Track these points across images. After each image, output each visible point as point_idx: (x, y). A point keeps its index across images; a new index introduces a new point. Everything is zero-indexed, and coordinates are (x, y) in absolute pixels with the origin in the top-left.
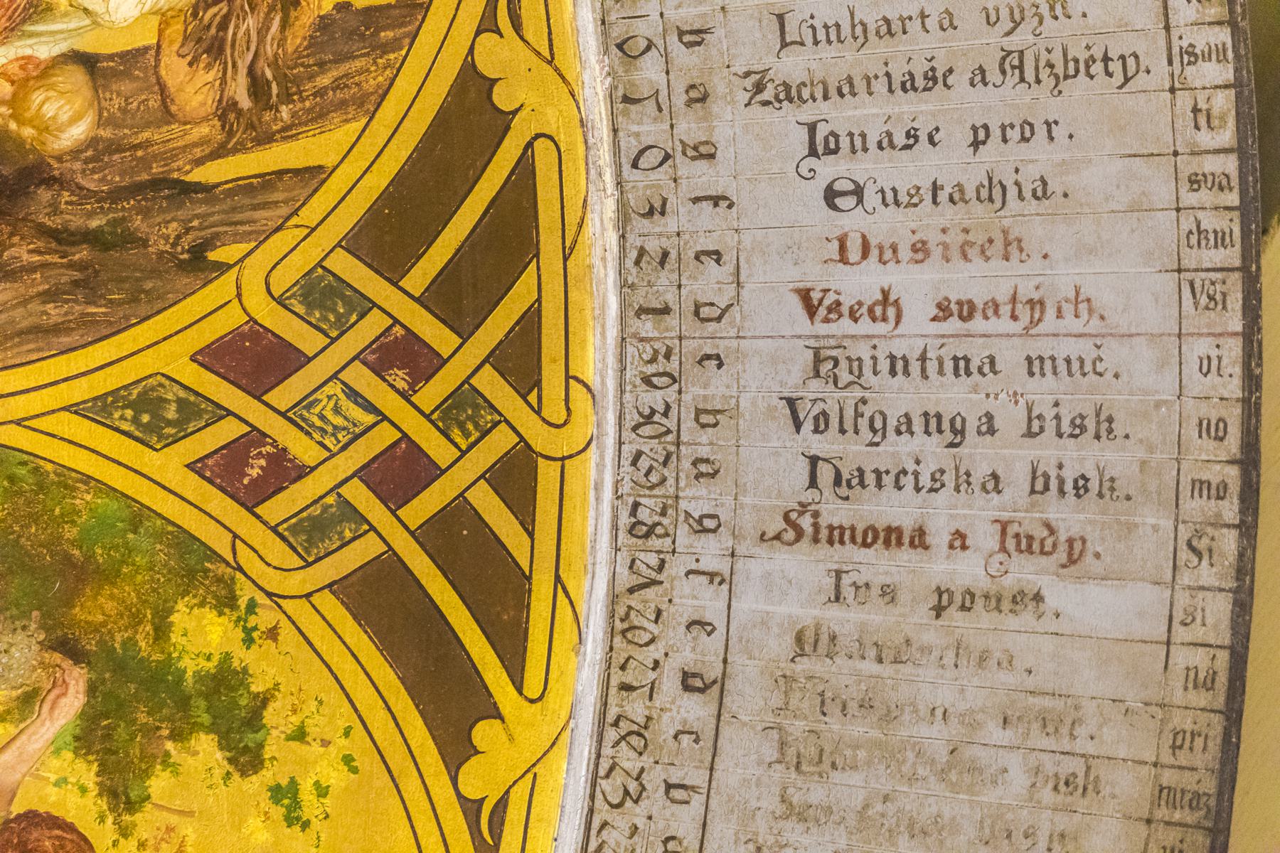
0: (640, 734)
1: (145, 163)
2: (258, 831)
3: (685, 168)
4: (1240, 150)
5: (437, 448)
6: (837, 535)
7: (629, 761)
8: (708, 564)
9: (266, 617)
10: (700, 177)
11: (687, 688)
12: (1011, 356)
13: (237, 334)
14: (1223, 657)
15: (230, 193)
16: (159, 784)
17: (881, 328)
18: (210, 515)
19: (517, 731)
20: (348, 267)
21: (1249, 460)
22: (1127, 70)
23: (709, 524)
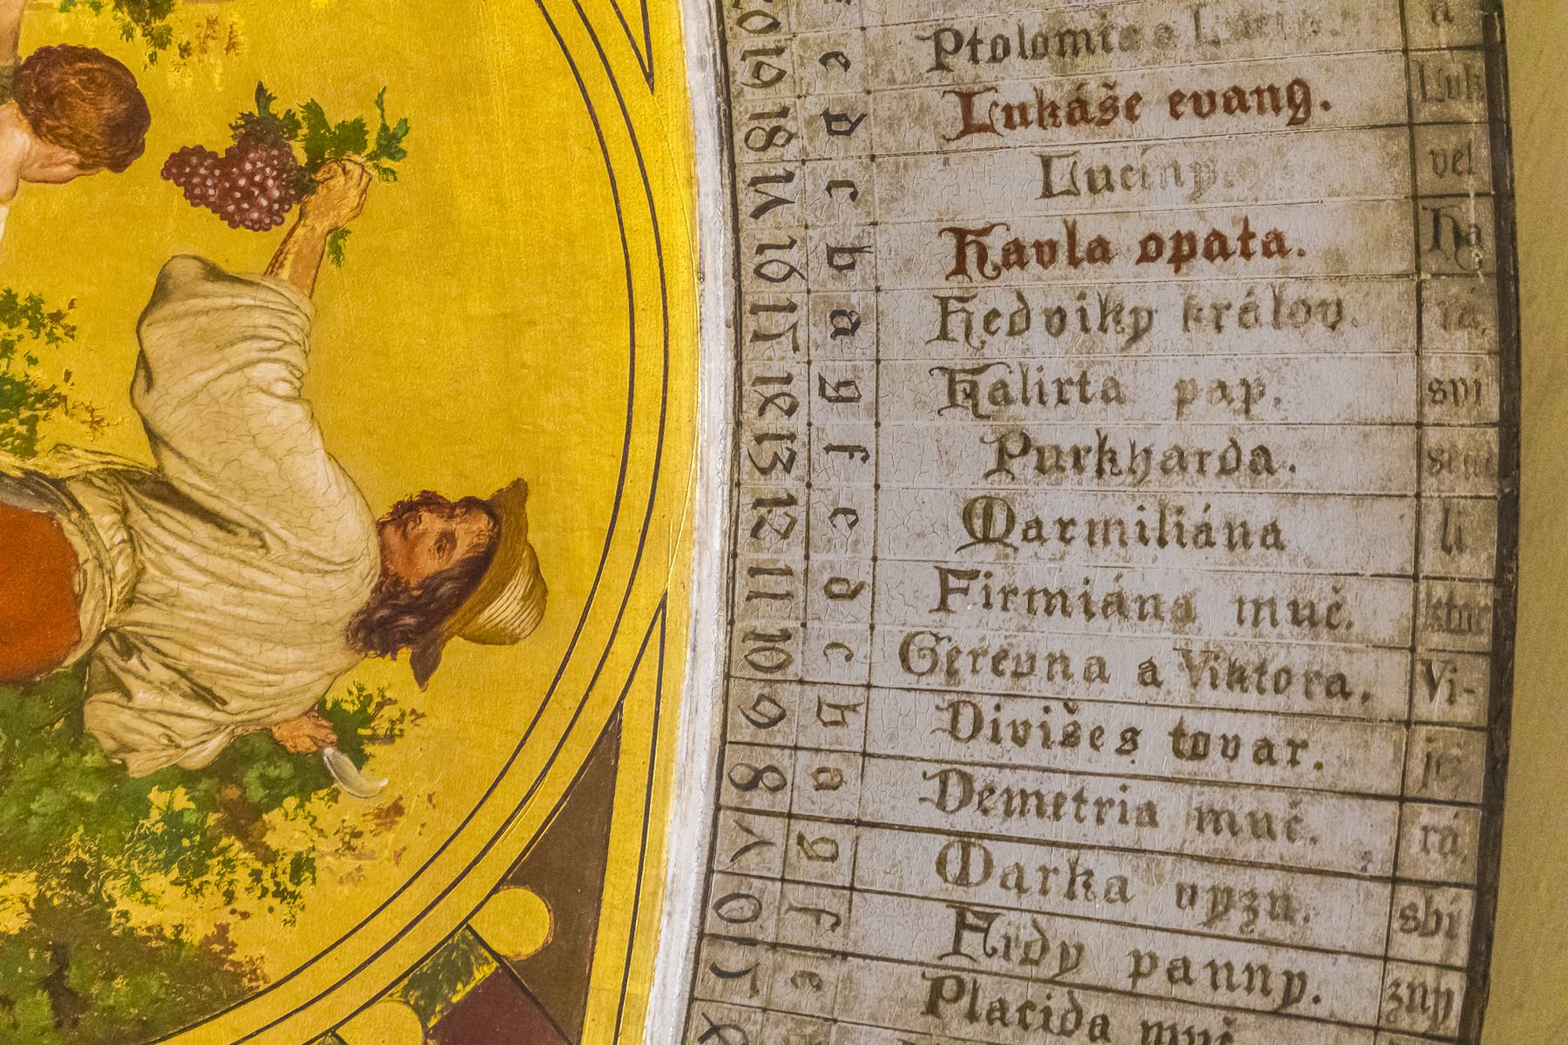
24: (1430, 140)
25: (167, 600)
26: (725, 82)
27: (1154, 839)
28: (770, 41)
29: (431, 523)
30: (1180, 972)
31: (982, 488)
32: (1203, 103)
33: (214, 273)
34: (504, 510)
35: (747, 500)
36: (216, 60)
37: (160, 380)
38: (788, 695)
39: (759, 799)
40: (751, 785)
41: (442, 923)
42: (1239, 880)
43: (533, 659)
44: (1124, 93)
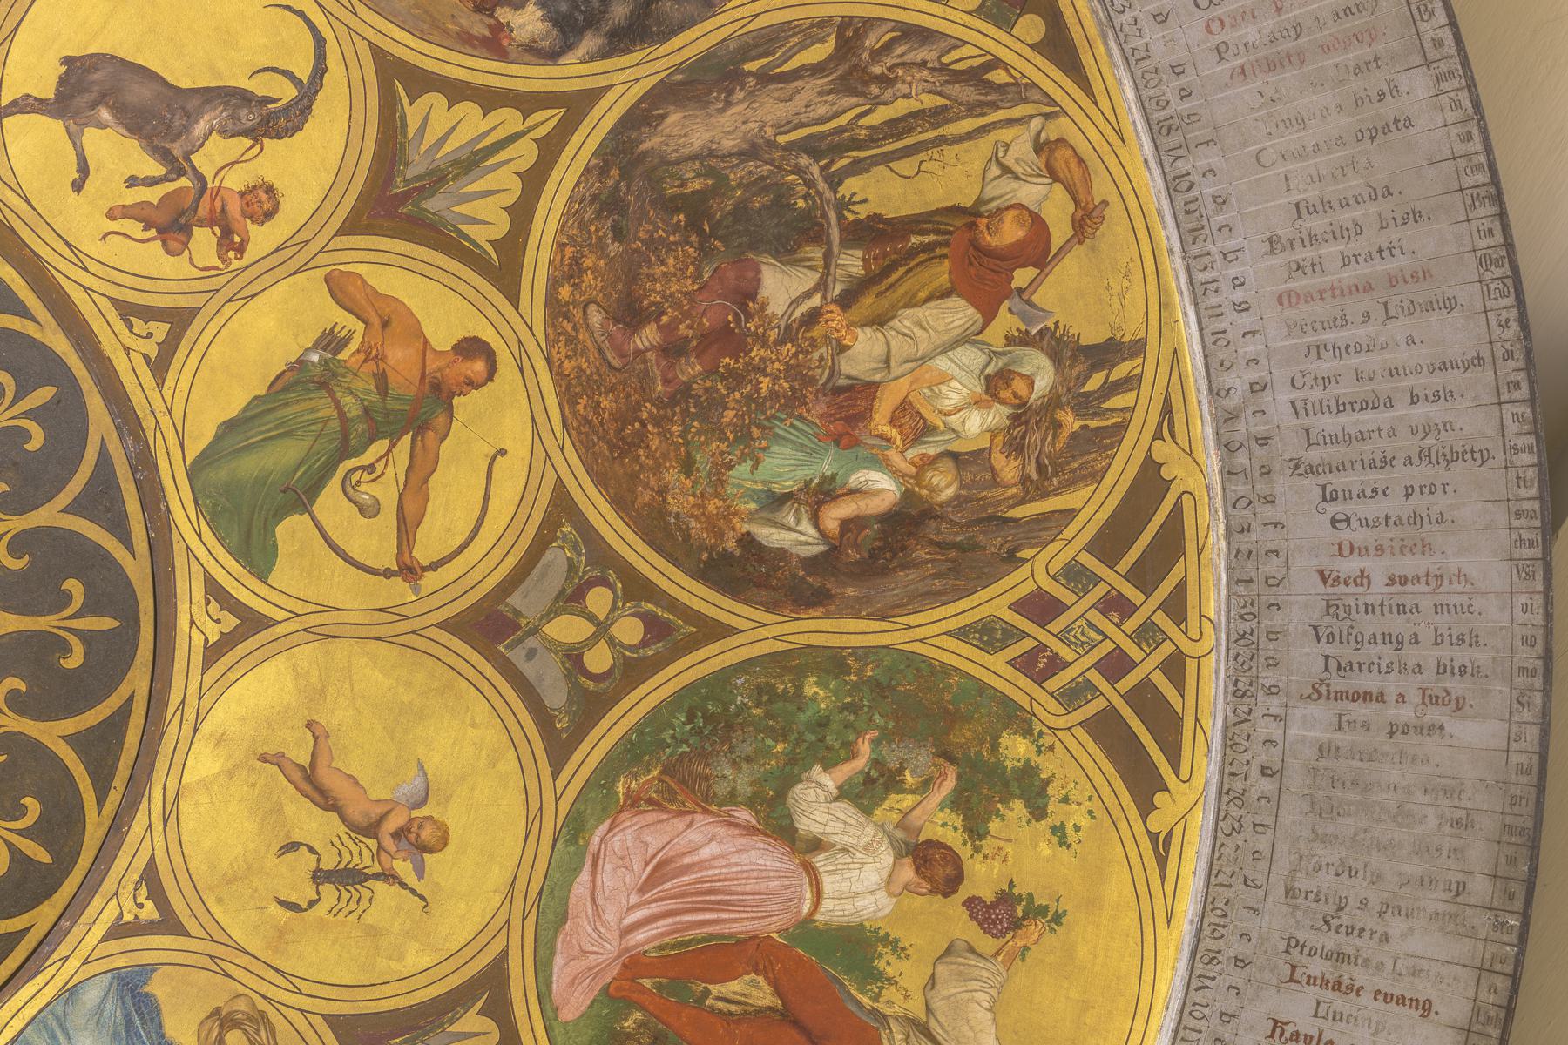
0: (1240, 798)
1: (984, 508)
2: (1045, 849)
4: (1541, 498)
5: (1134, 652)
6: (1339, 696)
7: (1235, 812)
8: (1273, 711)
9: (1047, 740)
10: (1267, 512)
11: (1263, 774)
12: (1426, 603)
13: (1032, 595)
14: (1536, 758)
16: (994, 825)
17: (1360, 590)
18: (1018, 687)
19: (1177, 797)
20: (1086, 559)
21: (1547, 656)
22: (1484, 458)
23: (1274, 690)
26: (1199, 932)
28: (1222, 921)
32: (1388, 997)
33: (971, 950)
36: (997, 864)
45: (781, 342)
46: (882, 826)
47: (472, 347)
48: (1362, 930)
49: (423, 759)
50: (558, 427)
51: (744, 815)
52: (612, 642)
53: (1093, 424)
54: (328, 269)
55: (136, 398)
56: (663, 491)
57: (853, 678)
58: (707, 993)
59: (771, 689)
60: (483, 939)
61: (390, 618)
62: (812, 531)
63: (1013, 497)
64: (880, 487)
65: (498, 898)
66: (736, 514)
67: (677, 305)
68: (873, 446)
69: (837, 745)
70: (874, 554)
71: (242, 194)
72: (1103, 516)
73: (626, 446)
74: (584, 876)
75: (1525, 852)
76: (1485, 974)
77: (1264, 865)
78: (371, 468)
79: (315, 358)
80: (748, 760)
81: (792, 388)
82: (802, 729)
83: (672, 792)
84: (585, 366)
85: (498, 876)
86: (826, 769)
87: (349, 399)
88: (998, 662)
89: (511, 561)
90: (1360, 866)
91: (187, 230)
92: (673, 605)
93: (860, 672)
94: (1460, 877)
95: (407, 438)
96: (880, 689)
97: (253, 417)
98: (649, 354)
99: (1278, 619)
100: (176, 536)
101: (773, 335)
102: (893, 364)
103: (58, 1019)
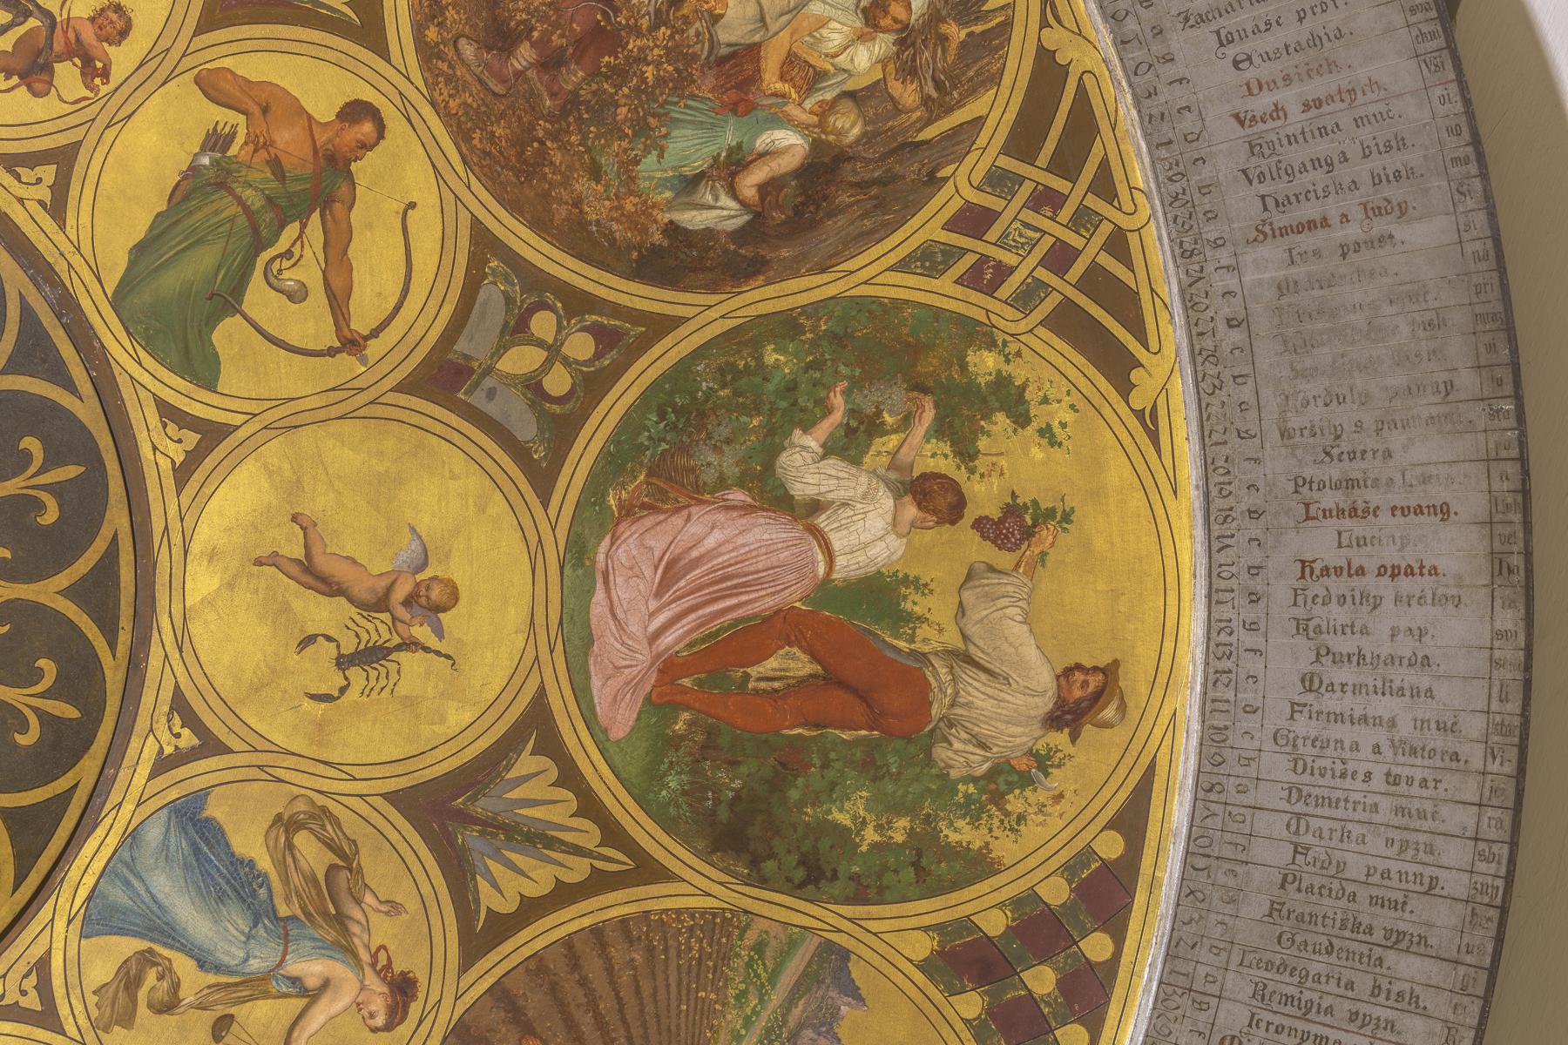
0: (1213, 355)
2: (1037, 454)
3: (1161, 69)
5: (1075, 241)
6: (1284, 231)
7: (1212, 370)
8: (1224, 262)
9: (1013, 347)
10: (1169, 71)
11: (1230, 326)
12: (1346, 120)
13: (961, 210)
14: (1489, 243)
15: (939, 142)
16: (983, 443)
17: (1279, 123)
18: (971, 304)
20: (1005, 162)
21: (1476, 141)
24: (1499, 529)
25: (968, 705)
26: (1207, 495)
27: (1377, 818)
28: (1226, 479)
29: (1079, 677)
30: (1386, 874)
31: (1310, 669)
32: (1405, 511)
33: (991, 569)
34: (1109, 673)
35: (1211, 670)
36: (995, 480)
37: (968, 613)
38: (1227, 753)
39: (1213, 796)
40: (1210, 790)
41: (1079, 844)
42: (1412, 837)
43: (1119, 735)
44: (1372, 506)
45: (655, 27)
46: (874, 472)
47: (355, 111)
48: (1365, 452)
49: (413, 523)
50: (460, 168)
51: (738, 496)
52: (566, 362)
53: (978, 29)
54: (196, 71)
55: (42, 245)
56: (577, 203)
57: (809, 336)
58: (747, 676)
59: (733, 365)
60: (517, 681)
61: (345, 394)
62: (733, 204)
63: (919, 119)
64: (787, 144)
65: (521, 638)
66: (654, 206)
67: (544, 18)
68: (770, 106)
69: (810, 405)
70: (798, 211)
71: (92, 20)
72: (1011, 115)
73: (530, 168)
74: (600, 595)
75: (1502, 336)
76: (1493, 464)
77: (1253, 414)
78: (288, 254)
79: (206, 161)
80: (728, 442)
81: (676, 70)
82: (772, 398)
83: (663, 492)
84: (470, 101)
85: (515, 616)
86: (805, 431)
87: (249, 192)
88: (945, 283)
89: (448, 309)
90: (1346, 391)
91: (48, 69)
92: (616, 310)
93: (814, 329)
94: (1445, 376)
95: (316, 216)
96: (838, 339)
97: (162, 233)
98: (529, 73)
99: (1206, 172)
100: (117, 370)
101: (645, 23)
102: (768, 20)
103: (128, 866)
